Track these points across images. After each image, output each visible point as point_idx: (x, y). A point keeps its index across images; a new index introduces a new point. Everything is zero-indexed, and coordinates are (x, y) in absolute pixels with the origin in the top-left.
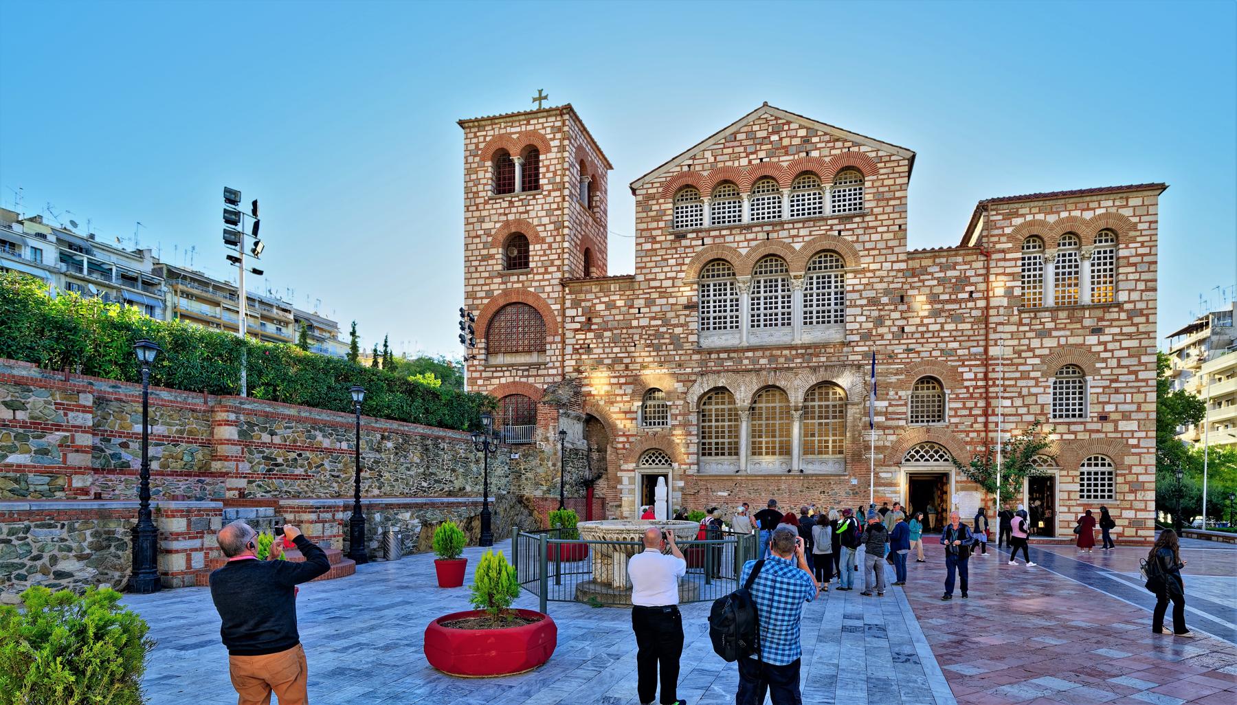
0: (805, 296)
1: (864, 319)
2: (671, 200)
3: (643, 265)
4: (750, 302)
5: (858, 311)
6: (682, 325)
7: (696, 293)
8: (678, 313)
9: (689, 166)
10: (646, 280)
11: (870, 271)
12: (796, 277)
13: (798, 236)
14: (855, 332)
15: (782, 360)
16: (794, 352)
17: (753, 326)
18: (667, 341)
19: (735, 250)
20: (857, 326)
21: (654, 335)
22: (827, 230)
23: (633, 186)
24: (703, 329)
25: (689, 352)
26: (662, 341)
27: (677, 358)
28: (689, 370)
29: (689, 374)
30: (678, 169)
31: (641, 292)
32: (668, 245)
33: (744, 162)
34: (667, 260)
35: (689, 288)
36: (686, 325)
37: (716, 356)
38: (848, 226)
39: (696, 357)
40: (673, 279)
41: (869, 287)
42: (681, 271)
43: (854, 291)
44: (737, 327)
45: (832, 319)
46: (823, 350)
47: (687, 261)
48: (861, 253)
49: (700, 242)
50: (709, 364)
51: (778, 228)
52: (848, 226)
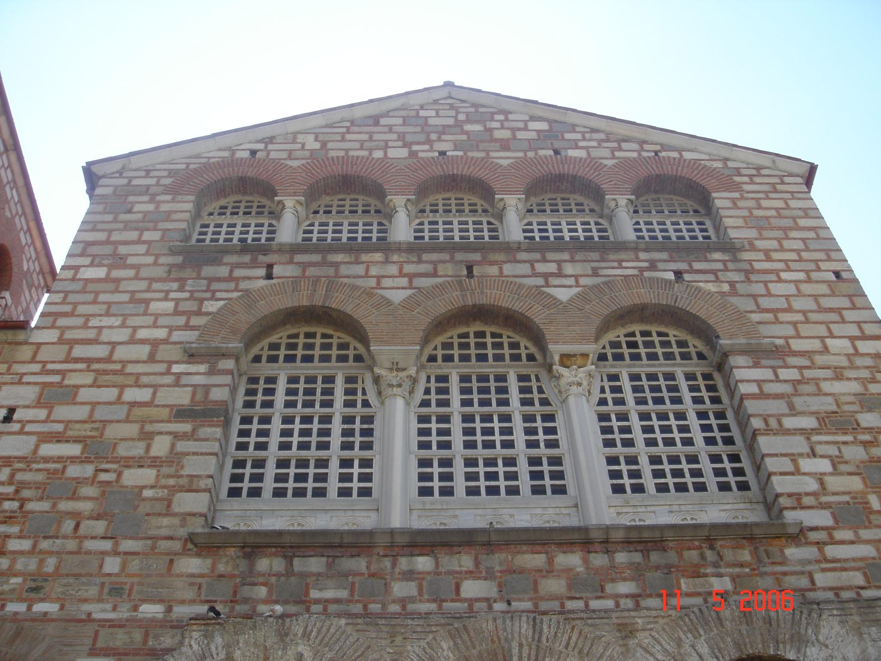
0: (603, 417)
1: (824, 466)
2: (192, 198)
3: (67, 308)
4: (415, 426)
5: (799, 444)
6: (155, 463)
7: (227, 379)
8: (148, 428)
9: (253, 153)
10: (61, 341)
11: (795, 354)
12: (566, 359)
13: (560, 274)
14: (806, 501)
15: (554, 586)
16: (599, 560)
17: (425, 492)
18: (86, 507)
19: (369, 293)
20: (812, 485)
21: (38, 486)
22: (642, 270)
23: (94, 169)
24: (234, 493)
25: (164, 545)
26: (65, 506)
27: (112, 565)
28: (151, 610)
29: (149, 626)
30: (226, 154)
31: (36, 368)
32: (160, 272)
33: (398, 153)
34: (147, 302)
35: (202, 368)
36: (175, 458)
37: (278, 564)
38: (697, 266)
39: (193, 565)
40: (155, 344)
41: (810, 388)
42: (187, 327)
43: (762, 395)
44: (365, 492)
45: (711, 480)
46: (710, 555)
47: (212, 306)
48: (755, 317)
49: (262, 272)
50: (246, 591)
51: (500, 257)
52: (697, 266)
